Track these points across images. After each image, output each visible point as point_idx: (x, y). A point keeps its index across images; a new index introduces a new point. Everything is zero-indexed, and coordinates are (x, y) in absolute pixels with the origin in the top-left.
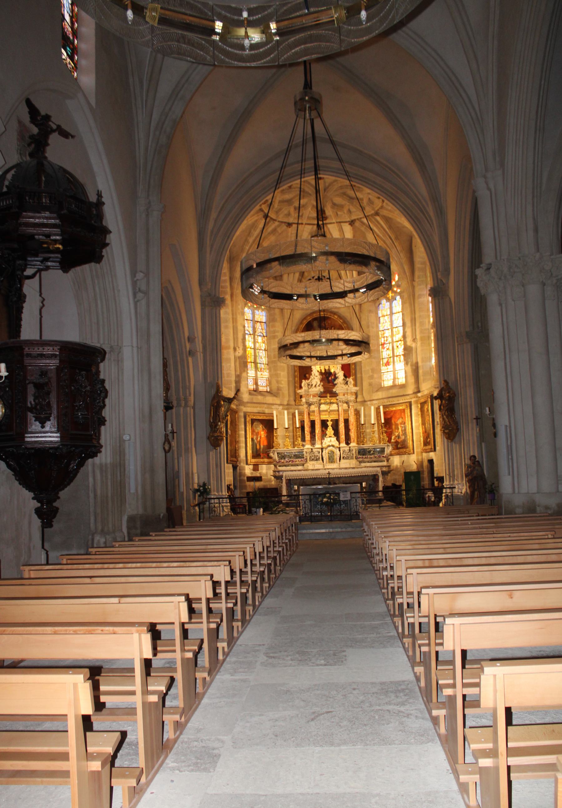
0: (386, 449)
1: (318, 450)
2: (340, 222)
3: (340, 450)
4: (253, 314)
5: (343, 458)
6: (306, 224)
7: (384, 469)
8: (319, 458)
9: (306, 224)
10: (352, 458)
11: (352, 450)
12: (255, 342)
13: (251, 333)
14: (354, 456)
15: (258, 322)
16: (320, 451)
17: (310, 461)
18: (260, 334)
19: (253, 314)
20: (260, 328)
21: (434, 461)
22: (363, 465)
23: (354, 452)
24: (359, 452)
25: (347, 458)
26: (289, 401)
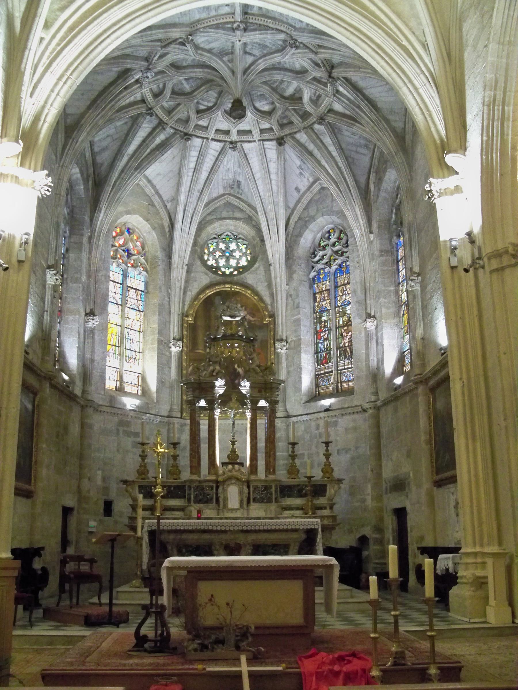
0: (328, 488)
1: (211, 484)
2: (263, 140)
3: (248, 487)
4: (125, 276)
5: (254, 500)
6: (212, 139)
7: (326, 522)
8: (212, 499)
9: (212, 139)
10: (269, 501)
11: (271, 487)
12: (123, 317)
13: (120, 303)
14: (274, 497)
15: (132, 288)
16: (214, 485)
17: (195, 503)
18: (133, 306)
19: (125, 276)
20: (135, 297)
21: (408, 509)
22: (287, 513)
23: (273, 490)
24: (281, 492)
25: (261, 501)
26: (171, 411)
